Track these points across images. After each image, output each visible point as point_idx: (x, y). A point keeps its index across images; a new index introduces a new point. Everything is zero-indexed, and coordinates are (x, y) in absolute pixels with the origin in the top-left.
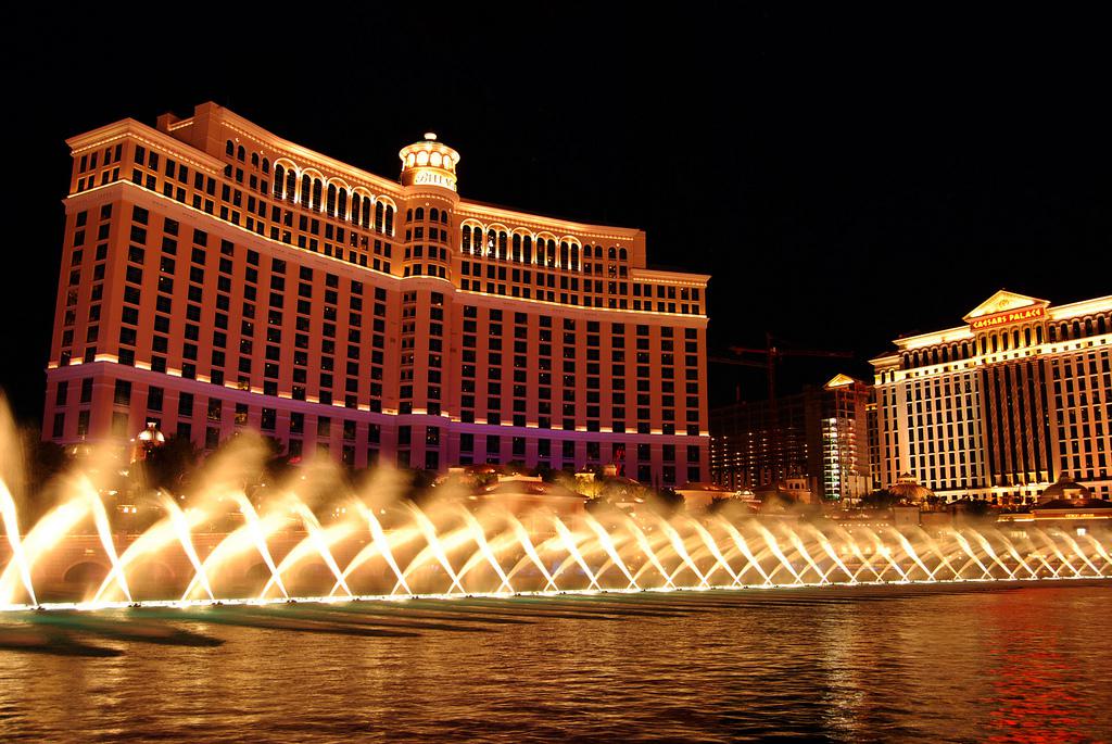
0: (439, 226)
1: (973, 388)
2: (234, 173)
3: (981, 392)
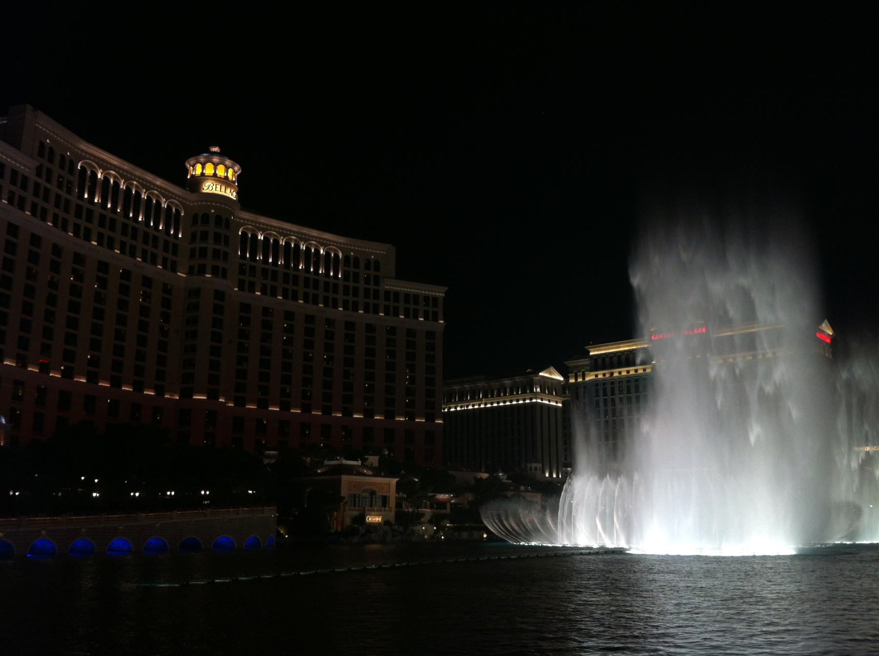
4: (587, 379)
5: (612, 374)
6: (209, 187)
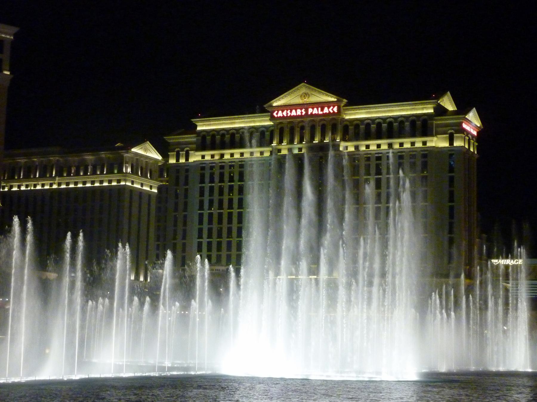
4: (191, 160)
5: (222, 156)
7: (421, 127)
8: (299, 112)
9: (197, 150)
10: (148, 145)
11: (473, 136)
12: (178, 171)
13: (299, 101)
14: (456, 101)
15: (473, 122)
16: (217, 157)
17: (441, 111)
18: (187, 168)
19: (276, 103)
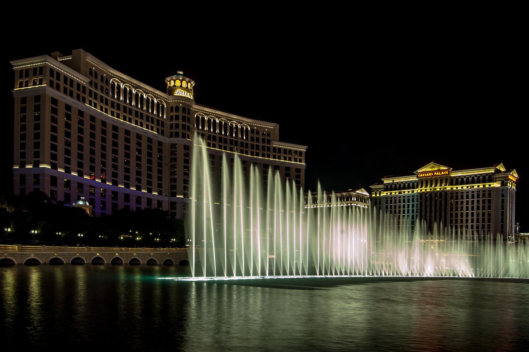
0: (186, 115)
1: (415, 200)
2: (93, 84)
3: (419, 203)
4: (382, 195)
5: (391, 193)
6: (179, 93)
7: (490, 178)
8: (430, 174)
9: (384, 191)
10: (363, 189)
11: (514, 182)
12: (376, 199)
13: (430, 170)
14: (505, 166)
15: (514, 176)
16: (389, 194)
17: (498, 171)
18: (380, 198)
19: (419, 171)
